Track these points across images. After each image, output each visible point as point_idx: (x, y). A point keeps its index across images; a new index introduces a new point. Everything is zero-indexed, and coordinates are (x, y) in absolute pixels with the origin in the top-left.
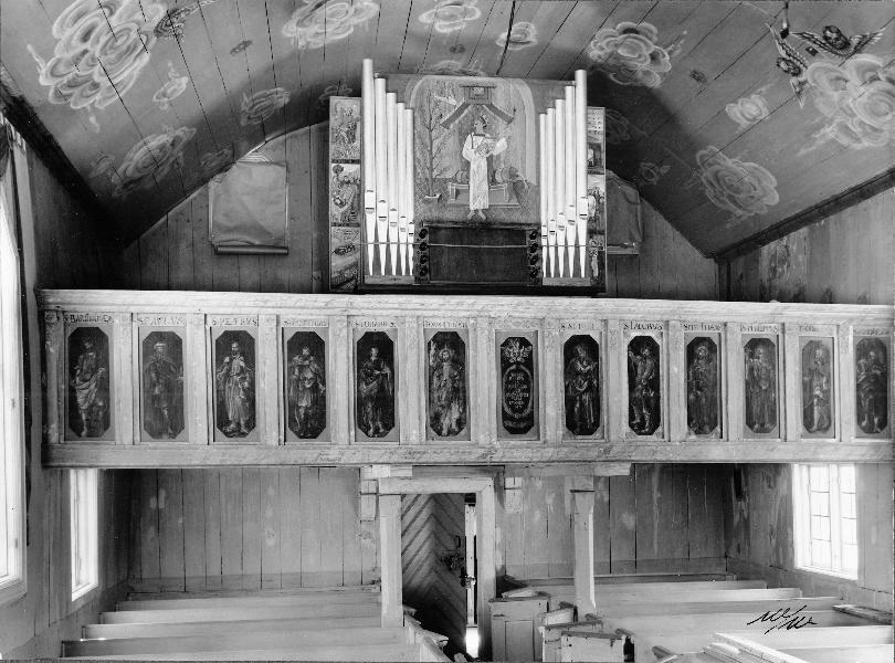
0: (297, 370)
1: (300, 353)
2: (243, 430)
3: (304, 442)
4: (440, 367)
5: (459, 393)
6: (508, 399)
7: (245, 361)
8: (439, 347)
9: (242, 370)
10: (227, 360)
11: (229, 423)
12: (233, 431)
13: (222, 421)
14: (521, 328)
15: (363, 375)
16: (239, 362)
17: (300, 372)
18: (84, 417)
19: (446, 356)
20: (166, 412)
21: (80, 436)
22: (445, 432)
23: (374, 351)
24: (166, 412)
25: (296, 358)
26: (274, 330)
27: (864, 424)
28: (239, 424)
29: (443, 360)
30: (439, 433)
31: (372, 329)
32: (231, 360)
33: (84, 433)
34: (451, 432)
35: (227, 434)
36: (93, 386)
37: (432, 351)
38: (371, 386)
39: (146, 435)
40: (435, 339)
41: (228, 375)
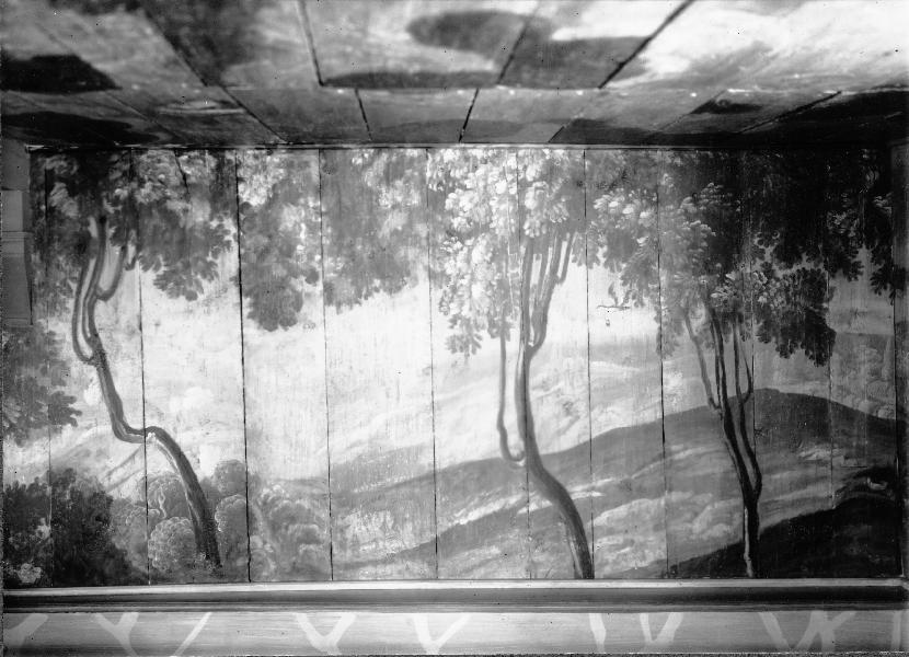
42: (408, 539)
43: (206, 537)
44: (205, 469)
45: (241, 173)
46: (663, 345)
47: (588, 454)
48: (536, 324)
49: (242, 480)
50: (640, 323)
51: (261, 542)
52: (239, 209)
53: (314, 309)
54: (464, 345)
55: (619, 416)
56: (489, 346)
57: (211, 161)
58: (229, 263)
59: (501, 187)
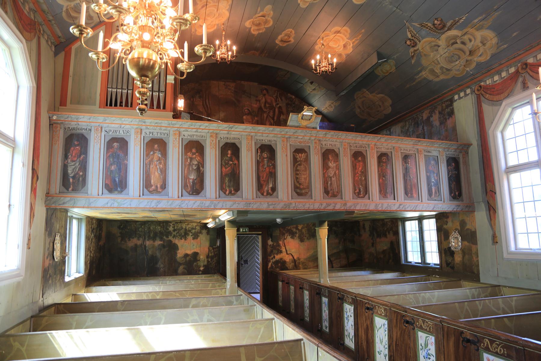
0: (189, 160)
1: (191, 151)
2: (159, 190)
3: (192, 198)
4: (263, 161)
5: (273, 175)
6: (297, 178)
7: (162, 154)
8: (262, 152)
9: (159, 159)
10: (152, 153)
11: (152, 186)
12: (154, 190)
13: (147, 185)
14: (302, 144)
15: (224, 164)
16: (158, 154)
17: (191, 161)
18: (71, 180)
19: (265, 156)
20: (117, 180)
21: (68, 190)
22: (265, 194)
23: (229, 152)
24: (117, 180)
25: (189, 154)
26: (178, 140)
27: (452, 195)
28: (157, 187)
29: (264, 158)
30: (263, 194)
31: (229, 141)
32: (154, 153)
33: (70, 189)
34: (268, 194)
35: (150, 192)
36: (78, 164)
37: (259, 154)
38: (228, 169)
39: (105, 191)
40: (260, 147)
41: (151, 161)
43: (295, 265)
44: (295, 258)
49: (299, 259)
50: (337, 241)
52: (298, 229)
53: (306, 240)
58: (297, 235)
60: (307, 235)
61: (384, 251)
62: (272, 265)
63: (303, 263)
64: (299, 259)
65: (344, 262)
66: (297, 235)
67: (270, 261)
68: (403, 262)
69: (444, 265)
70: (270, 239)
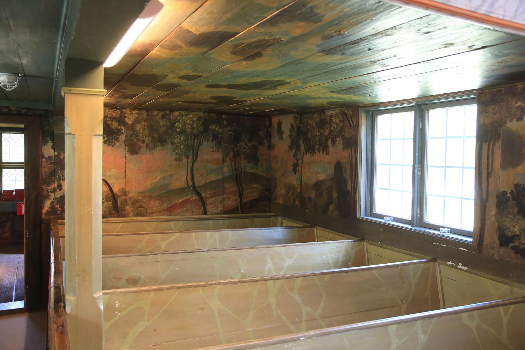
42: (165, 206)
43: (115, 206)
44: (116, 190)
45: (126, 115)
46: (224, 161)
47: (206, 186)
48: (195, 155)
49: (125, 193)
50: (218, 155)
51: (129, 208)
52: (124, 123)
53: (143, 150)
54: (179, 160)
55: (213, 177)
56: (185, 160)
57: (119, 112)
58: (122, 138)
59: (188, 122)
60: (148, 139)
61: (318, 185)
62: (52, 204)
63: (135, 202)
64: (125, 193)
65: (232, 202)
66: (122, 138)
67: (47, 197)
68: (362, 214)
69: (491, 238)
70: (50, 144)
